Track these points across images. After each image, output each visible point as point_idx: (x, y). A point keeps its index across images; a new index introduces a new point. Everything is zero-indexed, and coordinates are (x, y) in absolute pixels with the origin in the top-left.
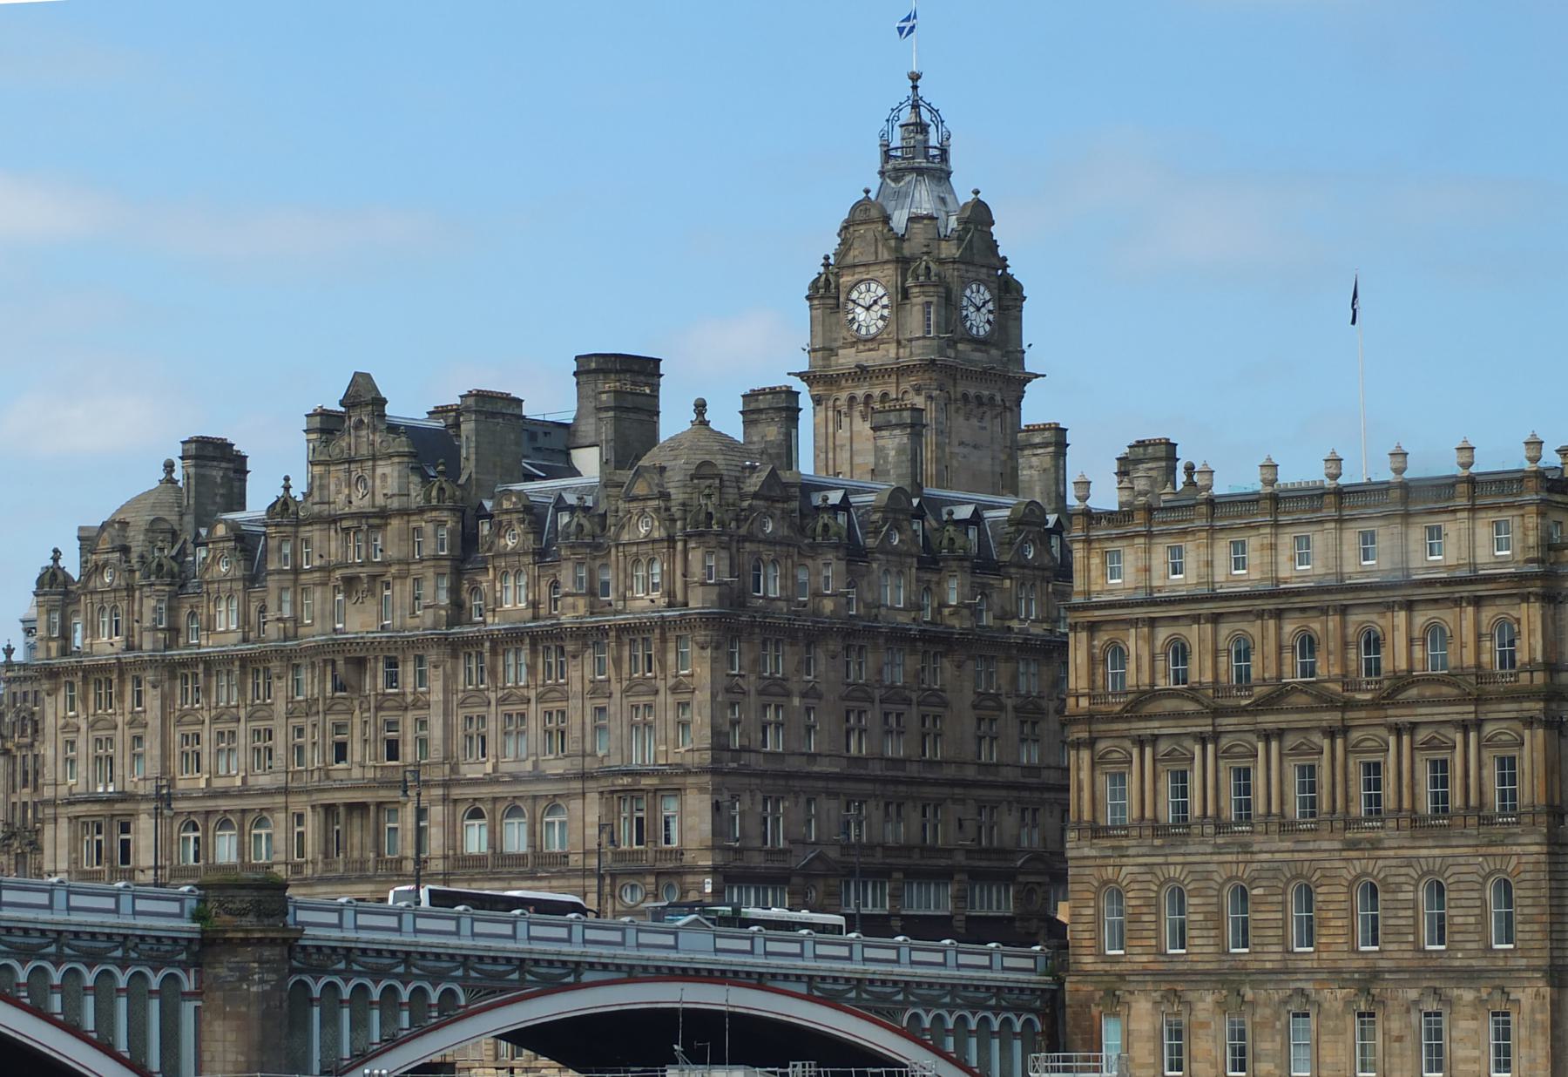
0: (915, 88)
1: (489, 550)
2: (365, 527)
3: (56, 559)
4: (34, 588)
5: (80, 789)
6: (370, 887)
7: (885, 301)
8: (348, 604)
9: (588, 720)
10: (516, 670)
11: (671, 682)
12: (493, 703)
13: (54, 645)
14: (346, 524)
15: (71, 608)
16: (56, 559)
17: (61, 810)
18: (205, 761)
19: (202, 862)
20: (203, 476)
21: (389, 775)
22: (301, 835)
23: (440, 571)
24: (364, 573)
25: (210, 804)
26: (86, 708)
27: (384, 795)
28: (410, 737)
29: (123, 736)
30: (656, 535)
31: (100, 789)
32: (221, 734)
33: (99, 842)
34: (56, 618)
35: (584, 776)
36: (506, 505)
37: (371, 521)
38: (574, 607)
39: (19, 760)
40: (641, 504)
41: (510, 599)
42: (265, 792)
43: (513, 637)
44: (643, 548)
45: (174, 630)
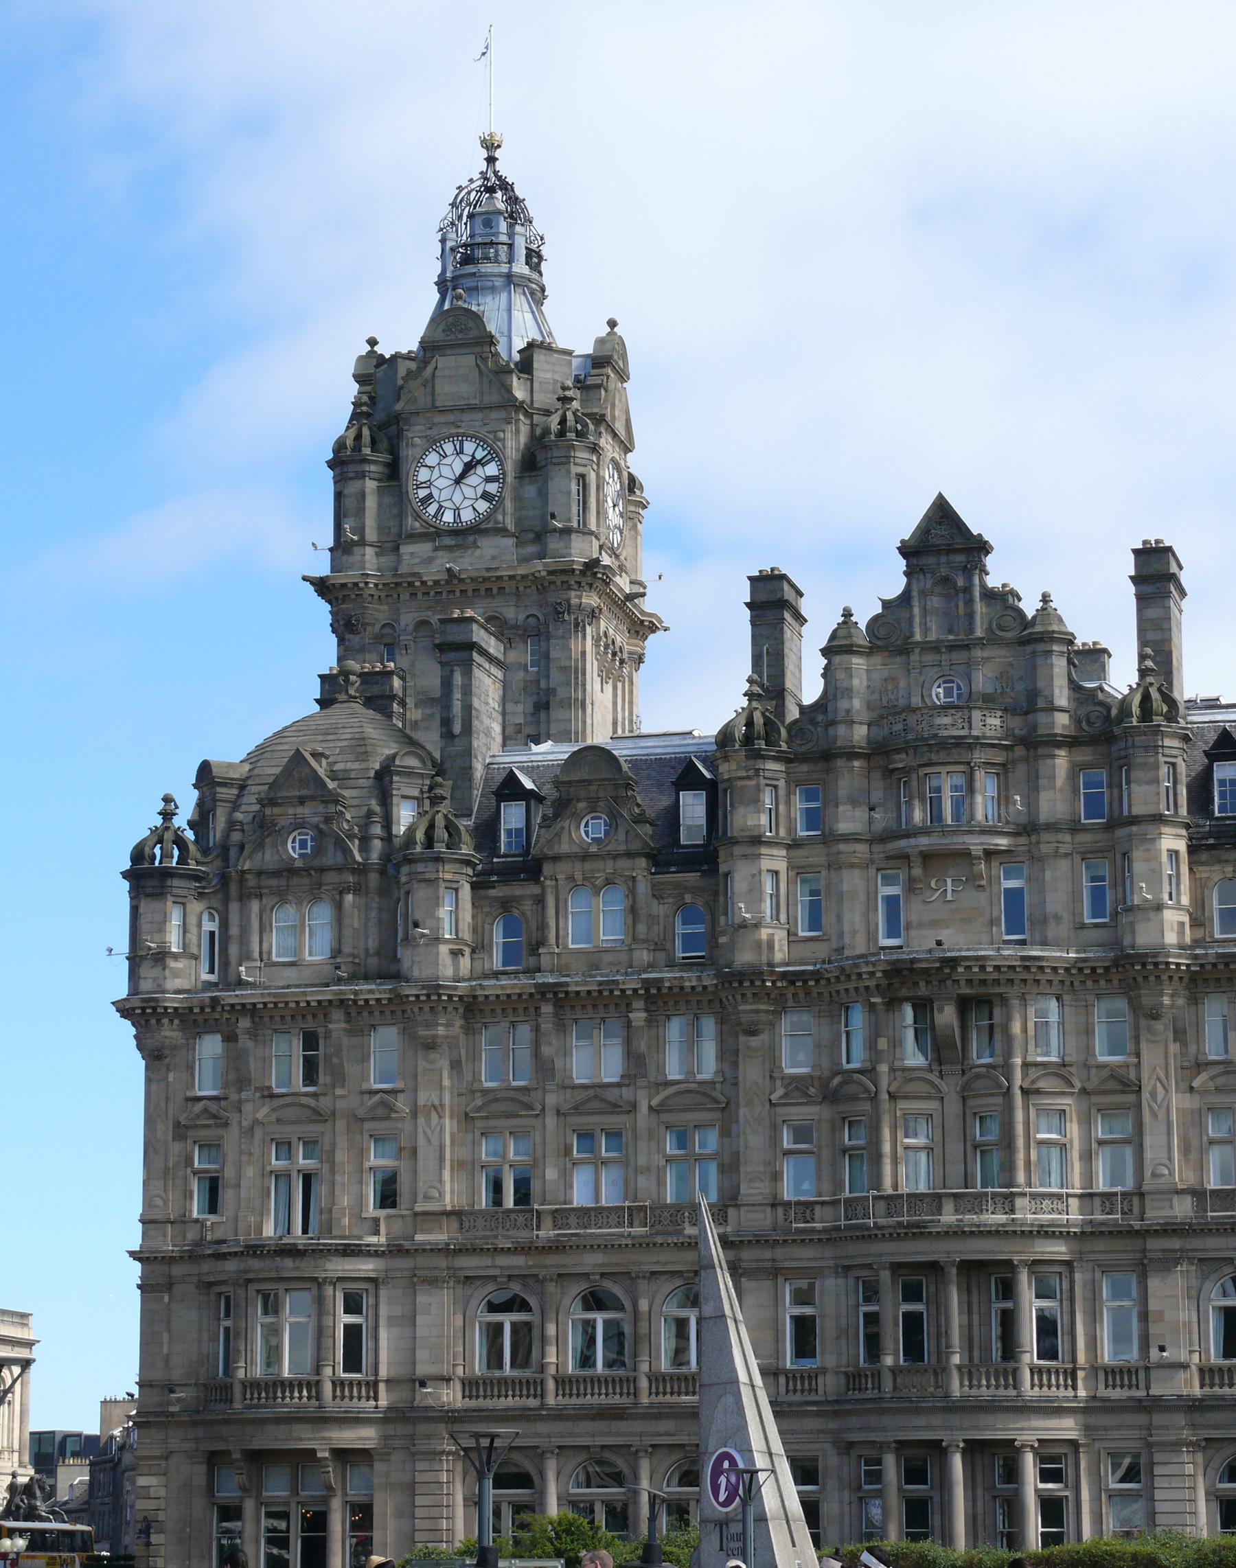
3: (167, 815)
4: (127, 865)
16: (167, 815)
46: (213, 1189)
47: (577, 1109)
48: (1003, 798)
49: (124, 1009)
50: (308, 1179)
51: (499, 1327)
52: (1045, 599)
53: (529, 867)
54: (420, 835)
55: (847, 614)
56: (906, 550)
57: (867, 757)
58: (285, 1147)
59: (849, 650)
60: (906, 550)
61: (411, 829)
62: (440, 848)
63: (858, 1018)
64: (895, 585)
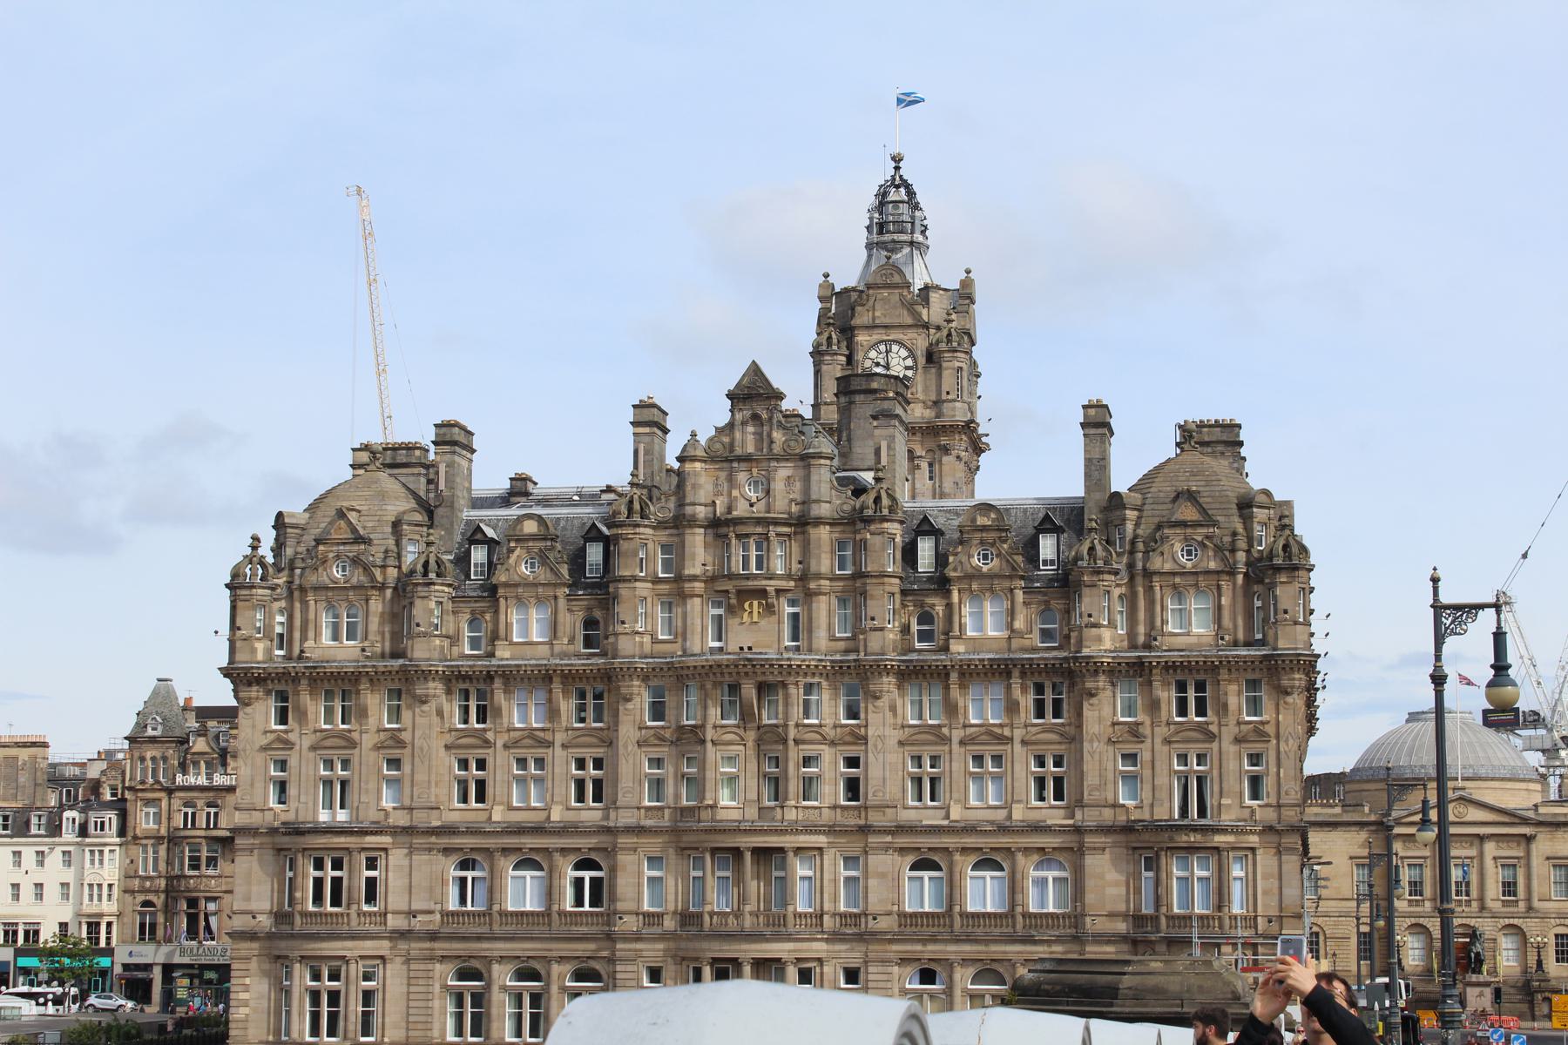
0: (897, 168)
3: (254, 548)
7: (909, 362)
12: (955, 740)
16: (254, 548)
21: (813, 816)
28: (828, 775)
31: (324, 816)
33: (337, 882)
36: (981, 521)
38: (1099, 639)
40: (1189, 531)
41: (982, 625)
43: (999, 671)
44: (1191, 580)
46: (282, 786)
48: (788, 557)
49: (227, 672)
50: (344, 784)
51: (463, 880)
53: (491, 592)
54: (419, 568)
55: (694, 435)
56: (730, 396)
57: (705, 527)
58: (329, 764)
59: (694, 459)
61: (415, 563)
62: (432, 575)
64: (723, 418)
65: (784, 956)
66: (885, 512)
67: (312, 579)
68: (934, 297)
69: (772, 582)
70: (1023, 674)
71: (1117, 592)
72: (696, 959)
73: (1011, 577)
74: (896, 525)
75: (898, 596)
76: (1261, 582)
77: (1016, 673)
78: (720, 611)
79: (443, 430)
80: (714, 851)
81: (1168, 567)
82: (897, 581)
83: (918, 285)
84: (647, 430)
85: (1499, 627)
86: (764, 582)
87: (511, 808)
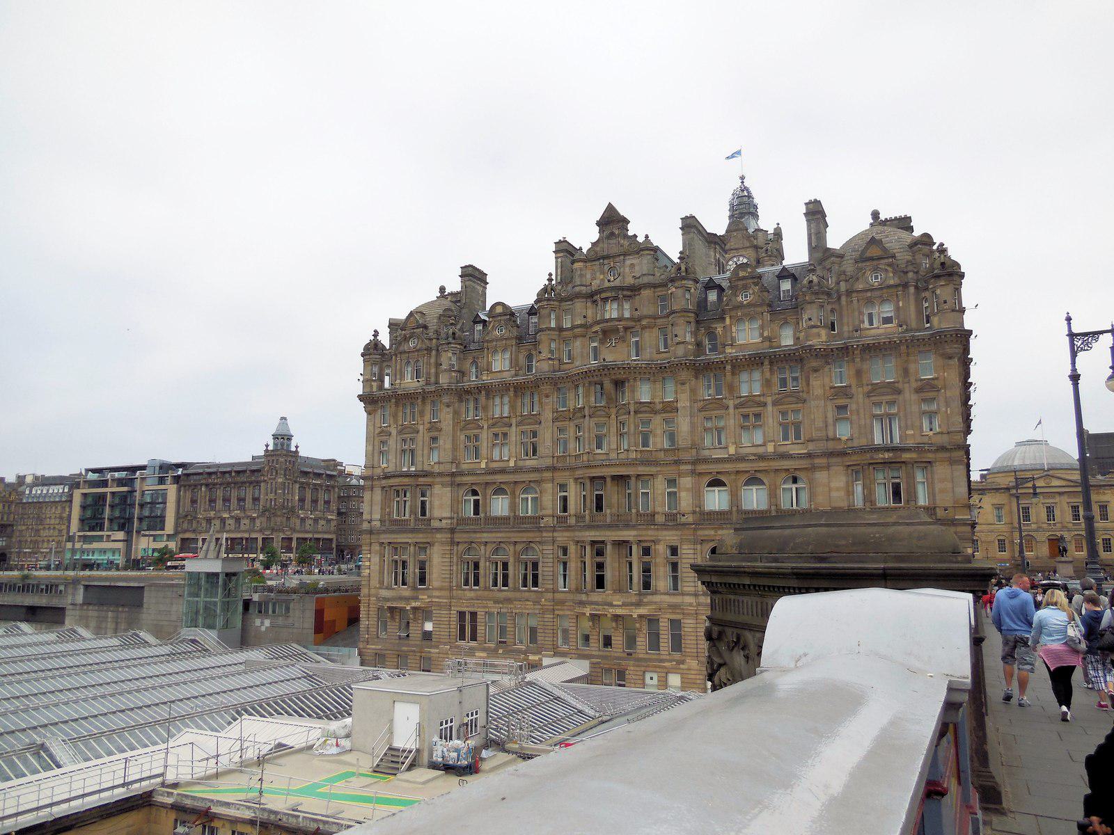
0: (743, 182)
1: (727, 305)
2: (621, 296)
5: (391, 469)
6: (634, 533)
8: (603, 348)
9: (830, 415)
10: (750, 385)
11: (914, 385)
13: (375, 384)
14: (604, 295)
15: (385, 364)
17: (376, 483)
18: (484, 451)
19: (482, 515)
20: (474, 287)
22: (565, 499)
23: (688, 319)
24: (621, 325)
25: (489, 478)
26: (396, 422)
27: (642, 470)
28: (659, 431)
29: (423, 436)
30: (892, 282)
32: (496, 435)
34: (376, 369)
35: (831, 454)
36: (741, 274)
37: (625, 293)
38: (819, 335)
39: (269, 484)
40: (875, 263)
41: (747, 336)
42: (536, 470)
44: (878, 293)
45: (462, 373)
47: (493, 425)
52: (647, 237)
56: (598, 224)
60: (598, 224)
63: (581, 390)
65: (631, 539)
66: (684, 274)
67: (401, 349)
68: (760, 234)
69: (621, 323)
70: (771, 363)
71: (829, 307)
72: (583, 542)
73: (761, 305)
74: (691, 282)
75: (693, 325)
76: (926, 289)
77: (766, 362)
78: (595, 344)
79: (466, 269)
80: (592, 479)
81: (860, 286)
82: (693, 315)
83: (751, 230)
84: (562, 254)
85: (1074, 369)
86: (617, 323)
87: (493, 461)
